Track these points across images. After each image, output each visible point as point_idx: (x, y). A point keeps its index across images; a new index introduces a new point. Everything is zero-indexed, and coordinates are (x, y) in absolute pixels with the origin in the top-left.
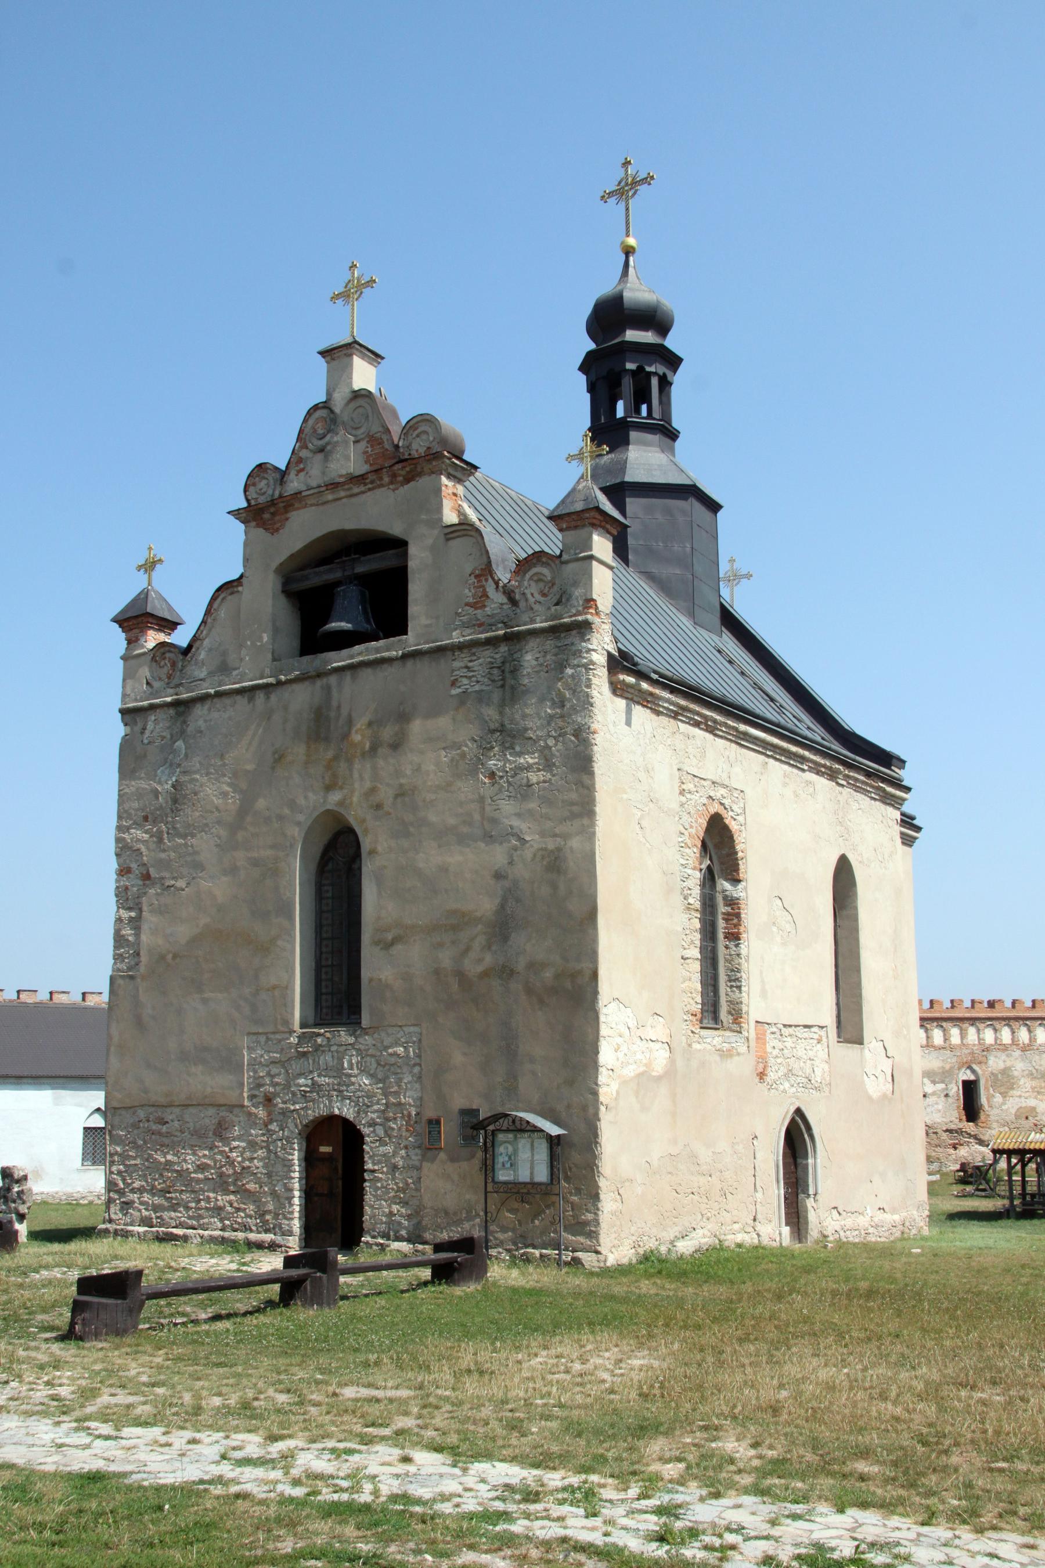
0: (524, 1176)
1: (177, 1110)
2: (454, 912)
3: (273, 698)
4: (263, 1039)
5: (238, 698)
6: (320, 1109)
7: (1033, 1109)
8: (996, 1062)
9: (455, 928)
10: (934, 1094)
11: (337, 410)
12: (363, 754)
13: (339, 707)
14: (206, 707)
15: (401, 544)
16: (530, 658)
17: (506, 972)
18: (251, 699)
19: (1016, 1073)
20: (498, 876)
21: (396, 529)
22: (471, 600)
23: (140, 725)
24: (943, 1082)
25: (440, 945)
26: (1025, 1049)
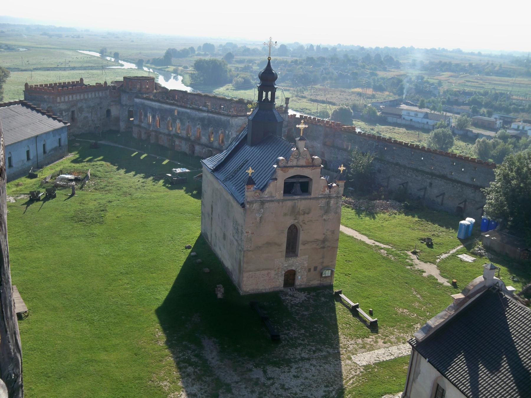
0: (327, 275)
1: (259, 272)
2: (316, 239)
3: (283, 203)
4: (278, 259)
5: (276, 203)
6: (290, 268)
7: (87, 117)
8: (79, 105)
9: (316, 242)
10: (65, 116)
11: (301, 152)
12: (302, 214)
13: (297, 206)
14: (269, 203)
15: (311, 180)
16: (332, 202)
17: (323, 248)
18: (279, 203)
19: (84, 107)
20: (324, 234)
21: (311, 177)
22: (322, 190)
23: (251, 206)
24: (67, 112)
25: (313, 244)
26: (86, 100)
